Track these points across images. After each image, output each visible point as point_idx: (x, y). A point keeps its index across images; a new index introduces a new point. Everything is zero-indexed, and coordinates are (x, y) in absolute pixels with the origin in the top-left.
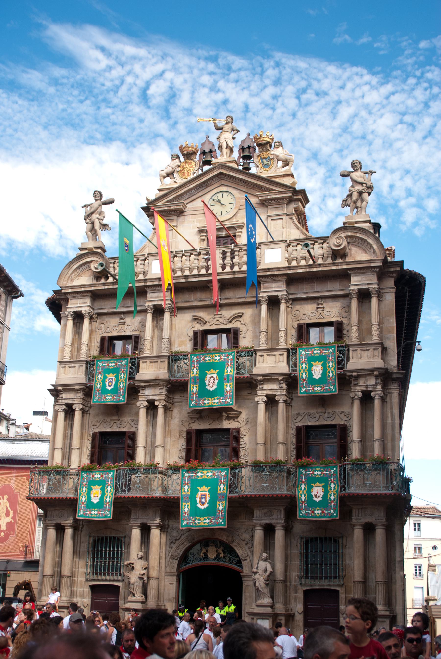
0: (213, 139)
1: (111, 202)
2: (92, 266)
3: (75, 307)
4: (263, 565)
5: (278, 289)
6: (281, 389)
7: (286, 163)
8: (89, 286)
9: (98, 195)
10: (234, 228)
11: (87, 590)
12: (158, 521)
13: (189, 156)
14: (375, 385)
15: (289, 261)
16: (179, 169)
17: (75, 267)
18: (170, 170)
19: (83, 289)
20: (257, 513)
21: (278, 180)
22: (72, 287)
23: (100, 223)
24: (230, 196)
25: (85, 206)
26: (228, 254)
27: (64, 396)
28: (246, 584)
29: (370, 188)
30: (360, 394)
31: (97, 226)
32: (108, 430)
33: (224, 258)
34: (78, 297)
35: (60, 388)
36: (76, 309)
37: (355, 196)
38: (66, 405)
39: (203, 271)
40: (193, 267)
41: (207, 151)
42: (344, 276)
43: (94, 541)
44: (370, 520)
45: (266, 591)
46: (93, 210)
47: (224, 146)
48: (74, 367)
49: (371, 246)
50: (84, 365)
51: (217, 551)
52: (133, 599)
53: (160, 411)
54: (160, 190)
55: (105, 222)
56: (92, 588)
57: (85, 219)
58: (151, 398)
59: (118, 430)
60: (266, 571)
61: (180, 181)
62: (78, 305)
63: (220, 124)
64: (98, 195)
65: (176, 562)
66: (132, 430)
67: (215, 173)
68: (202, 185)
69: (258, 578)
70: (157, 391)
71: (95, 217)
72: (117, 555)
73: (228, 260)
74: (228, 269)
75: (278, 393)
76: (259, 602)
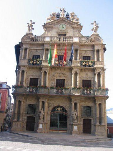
4: (75, 112)
9: (31, 21)
11: (26, 118)
14: (101, 71)
15: (80, 41)
20: (73, 100)
23: (32, 28)
24: (64, 25)
26: (65, 38)
29: (98, 27)
32: (33, 78)
33: (64, 39)
37: (94, 29)
39: (59, 41)
40: (56, 40)
43: (28, 105)
45: (76, 119)
50: (27, 61)
53: (47, 74)
54: (47, 22)
58: (45, 70)
60: (76, 114)
61: (52, 21)
64: (31, 21)
65: (50, 111)
68: (58, 22)
70: (47, 68)
76: (74, 122)
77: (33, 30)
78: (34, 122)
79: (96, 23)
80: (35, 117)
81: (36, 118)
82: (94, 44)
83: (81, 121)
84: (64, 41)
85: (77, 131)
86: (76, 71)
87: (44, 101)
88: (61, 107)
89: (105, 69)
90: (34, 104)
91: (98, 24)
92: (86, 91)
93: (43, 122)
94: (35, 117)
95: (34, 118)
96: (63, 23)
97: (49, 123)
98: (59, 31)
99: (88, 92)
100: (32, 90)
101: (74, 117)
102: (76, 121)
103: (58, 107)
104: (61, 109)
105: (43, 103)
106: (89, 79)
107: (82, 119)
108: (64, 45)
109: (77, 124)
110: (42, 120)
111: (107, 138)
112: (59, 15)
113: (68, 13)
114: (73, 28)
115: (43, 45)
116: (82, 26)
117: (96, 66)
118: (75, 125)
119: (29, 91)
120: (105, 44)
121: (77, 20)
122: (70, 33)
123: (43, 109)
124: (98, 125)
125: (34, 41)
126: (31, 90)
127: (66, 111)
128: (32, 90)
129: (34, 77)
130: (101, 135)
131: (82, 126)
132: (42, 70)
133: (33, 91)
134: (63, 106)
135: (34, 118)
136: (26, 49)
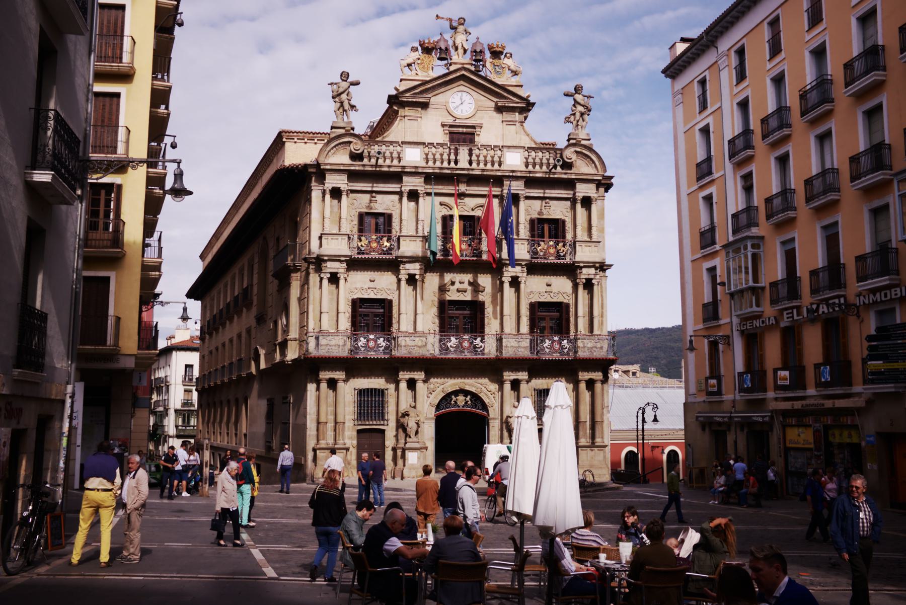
0: (447, 36)
1: (357, 84)
2: (352, 147)
5: (517, 187)
6: (523, 271)
7: (515, 73)
9: (345, 76)
10: (474, 127)
11: (355, 433)
13: (427, 50)
14: (596, 274)
16: (419, 62)
17: (333, 145)
18: (410, 61)
21: (510, 88)
22: (331, 164)
24: (469, 96)
25: (331, 84)
27: (329, 264)
29: (590, 111)
30: (584, 281)
31: (346, 106)
33: (470, 155)
35: (326, 258)
36: (334, 185)
38: (331, 273)
39: (452, 165)
41: (443, 48)
42: (570, 184)
46: (341, 90)
47: (460, 47)
49: (593, 162)
55: (353, 102)
56: (359, 432)
57: (333, 98)
58: (412, 272)
59: (375, 297)
63: (455, 24)
64: (345, 76)
65: (434, 409)
66: (389, 298)
67: (458, 74)
68: (445, 82)
71: (344, 96)
73: (474, 158)
74: (474, 165)
75: (520, 275)
77: (352, 113)
79: (585, 92)
82: (573, 177)
84: (470, 163)
86: (514, 274)
87: (416, 377)
88: (466, 393)
89: (611, 266)
90: (377, 387)
91: (589, 97)
92: (547, 343)
95: (383, 431)
96: (462, 88)
97: (431, 446)
98: (449, 120)
99: (557, 346)
100: (376, 342)
103: (456, 393)
104: (468, 399)
105: (412, 384)
106: (555, 300)
108: (472, 180)
112: (447, 49)
113: (478, 38)
114: (499, 109)
115: (396, 177)
116: (534, 104)
117: (584, 254)
120: (612, 177)
121: (515, 73)
122: (493, 130)
125: (366, 161)
128: (376, 342)
132: (402, 272)
134: (473, 390)
135: (383, 431)
136: (336, 193)
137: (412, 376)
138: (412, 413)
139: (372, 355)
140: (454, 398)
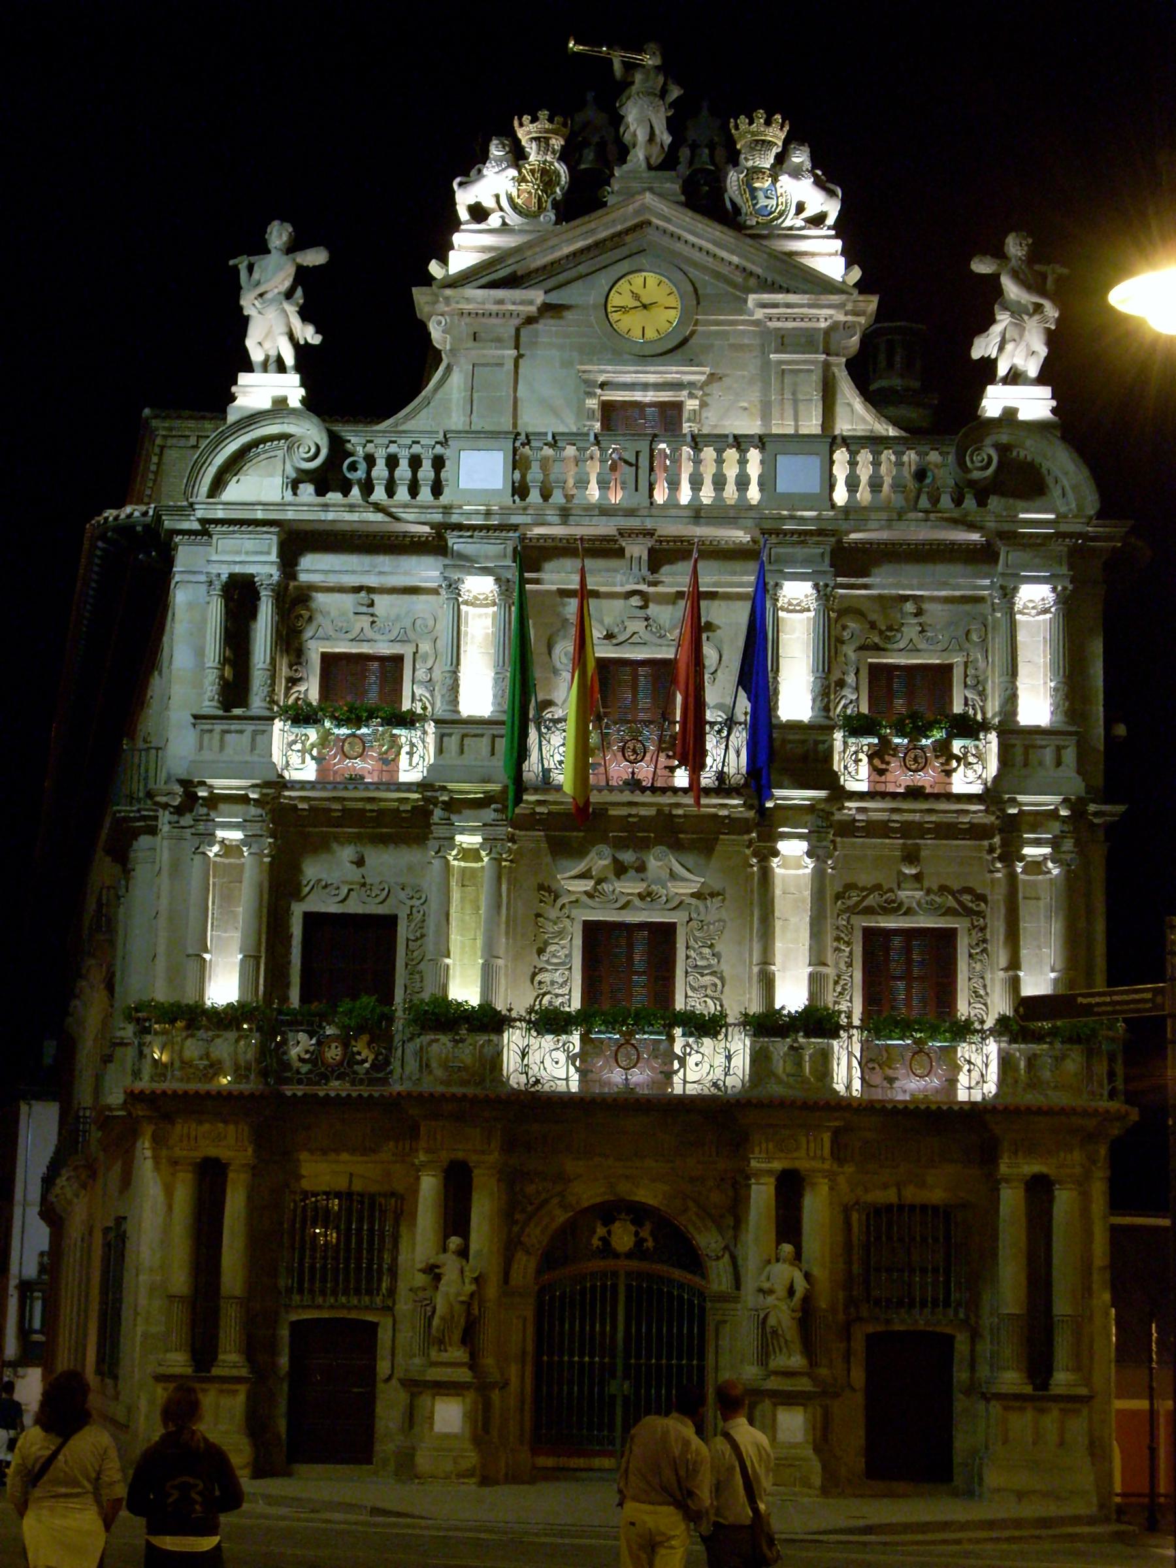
3: (235, 563)
8: (282, 505)
12: (494, 1157)
19: (260, 515)
28: (718, 1318)
34: (242, 533)
36: (237, 569)
44: (1044, 1169)
48: (241, 732)
51: (636, 1234)
52: (445, 1357)
62: (243, 558)
69: (775, 1306)
72: (371, 1243)
78: (368, 1375)
80: (375, 1326)
81: (384, 1336)
83: (847, 1356)
85: (809, 1452)
88: (638, 1213)
93: (463, 1375)
94: (375, 1326)
100: (346, 1045)
101: (772, 1321)
102: (796, 1361)
103: (608, 1212)
104: (645, 1233)
107: (859, 1335)
109: (804, 1385)
110: (458, 1354)
111: (1091, 1521)
118: (789, 1399)
119: (315, 1058)
123: (455, 1242)
124: (1017, 1397)
126: (334, 1053)
127: (693, 1261)
129: (354, 907)
130: (1046, 1495)
131: (851, 1408)
133: (350, 1059)
137: (460, 1155)
138: (451, 1266)
139: (336, 1087)
140: (601, 1231)
